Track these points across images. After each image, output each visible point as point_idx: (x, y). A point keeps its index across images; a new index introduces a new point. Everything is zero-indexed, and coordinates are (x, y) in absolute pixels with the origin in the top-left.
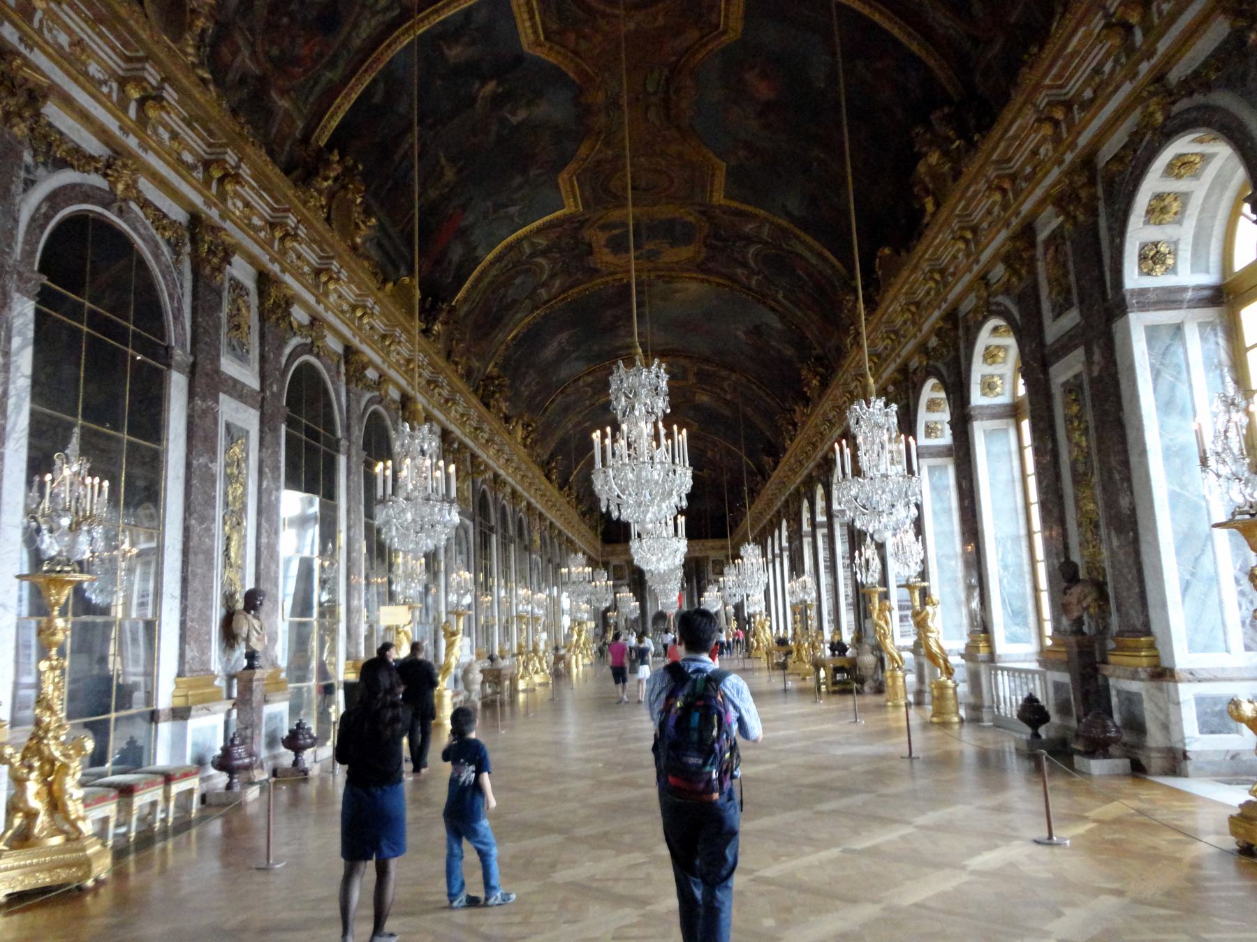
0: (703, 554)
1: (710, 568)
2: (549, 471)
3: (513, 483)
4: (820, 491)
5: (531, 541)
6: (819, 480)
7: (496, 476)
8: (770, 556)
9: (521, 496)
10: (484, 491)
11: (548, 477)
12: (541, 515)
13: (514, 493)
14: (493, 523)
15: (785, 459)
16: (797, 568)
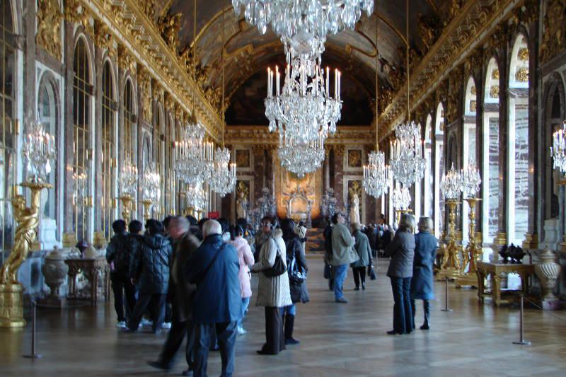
0: (339, 142)
1: (346, 159)
2: (167, 30)
3: (121, 37)
4: (492, 66)
5: (141, 110)
6: (493, 53)
7: (98, 25)
8: (428, 140)
9: (131, 55)
10: (81, 40)
11: (165, 37)
12: (154, 81)
13: (121, 49)
14: (92, 82)
15: (450, 28)
16: (453, 157)
